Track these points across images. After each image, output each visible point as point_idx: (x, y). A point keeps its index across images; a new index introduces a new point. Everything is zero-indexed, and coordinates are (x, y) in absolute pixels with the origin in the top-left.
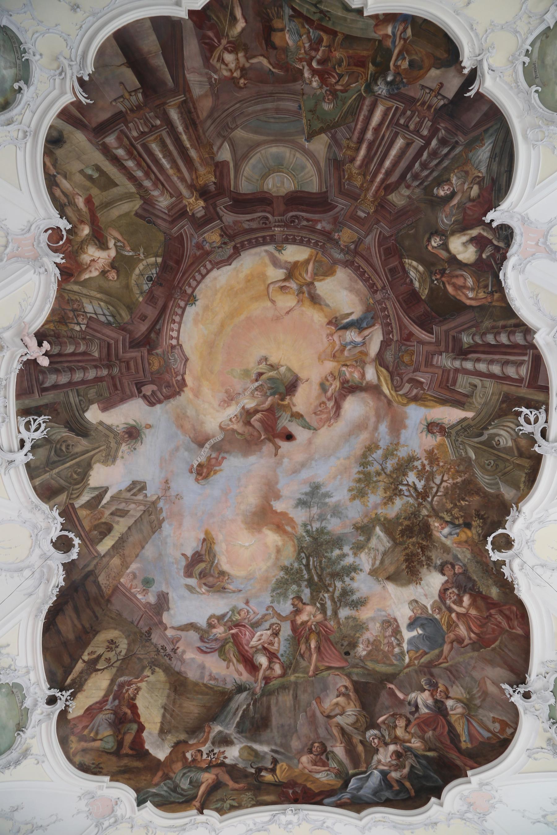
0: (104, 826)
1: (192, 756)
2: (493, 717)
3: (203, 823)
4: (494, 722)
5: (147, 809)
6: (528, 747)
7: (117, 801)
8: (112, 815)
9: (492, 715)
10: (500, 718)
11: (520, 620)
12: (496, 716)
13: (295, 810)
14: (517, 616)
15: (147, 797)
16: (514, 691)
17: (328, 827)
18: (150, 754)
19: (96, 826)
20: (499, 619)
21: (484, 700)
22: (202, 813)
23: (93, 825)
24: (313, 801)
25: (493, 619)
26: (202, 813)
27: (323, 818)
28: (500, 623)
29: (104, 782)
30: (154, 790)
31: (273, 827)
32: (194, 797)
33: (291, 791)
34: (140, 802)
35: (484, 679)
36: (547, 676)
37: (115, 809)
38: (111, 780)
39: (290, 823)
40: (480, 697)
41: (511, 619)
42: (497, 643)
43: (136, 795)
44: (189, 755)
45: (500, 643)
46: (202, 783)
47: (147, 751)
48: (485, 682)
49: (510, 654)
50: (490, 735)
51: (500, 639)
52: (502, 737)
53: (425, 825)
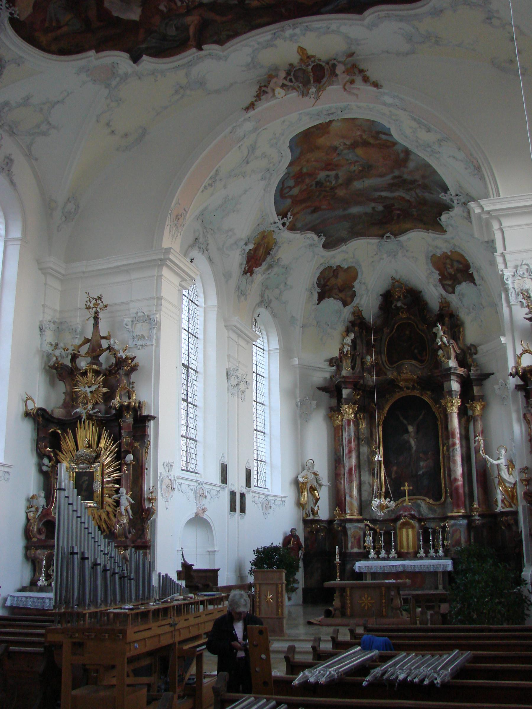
1: (166, 7)
3: (206, 56)
7: (114, 66)
13: (293, 25)
17: (333, 31)
18: (122, 19)
26: (201, 49)
29: (91, 56)
30: (144, 46)
31: (278, 42)
32: (188, 39)
33: (283, 10)
34: (136, 59)
38: (97, 52)
39: (295, 35)
44: (162, 7)
46: (189, 26)
47: (117, 18)
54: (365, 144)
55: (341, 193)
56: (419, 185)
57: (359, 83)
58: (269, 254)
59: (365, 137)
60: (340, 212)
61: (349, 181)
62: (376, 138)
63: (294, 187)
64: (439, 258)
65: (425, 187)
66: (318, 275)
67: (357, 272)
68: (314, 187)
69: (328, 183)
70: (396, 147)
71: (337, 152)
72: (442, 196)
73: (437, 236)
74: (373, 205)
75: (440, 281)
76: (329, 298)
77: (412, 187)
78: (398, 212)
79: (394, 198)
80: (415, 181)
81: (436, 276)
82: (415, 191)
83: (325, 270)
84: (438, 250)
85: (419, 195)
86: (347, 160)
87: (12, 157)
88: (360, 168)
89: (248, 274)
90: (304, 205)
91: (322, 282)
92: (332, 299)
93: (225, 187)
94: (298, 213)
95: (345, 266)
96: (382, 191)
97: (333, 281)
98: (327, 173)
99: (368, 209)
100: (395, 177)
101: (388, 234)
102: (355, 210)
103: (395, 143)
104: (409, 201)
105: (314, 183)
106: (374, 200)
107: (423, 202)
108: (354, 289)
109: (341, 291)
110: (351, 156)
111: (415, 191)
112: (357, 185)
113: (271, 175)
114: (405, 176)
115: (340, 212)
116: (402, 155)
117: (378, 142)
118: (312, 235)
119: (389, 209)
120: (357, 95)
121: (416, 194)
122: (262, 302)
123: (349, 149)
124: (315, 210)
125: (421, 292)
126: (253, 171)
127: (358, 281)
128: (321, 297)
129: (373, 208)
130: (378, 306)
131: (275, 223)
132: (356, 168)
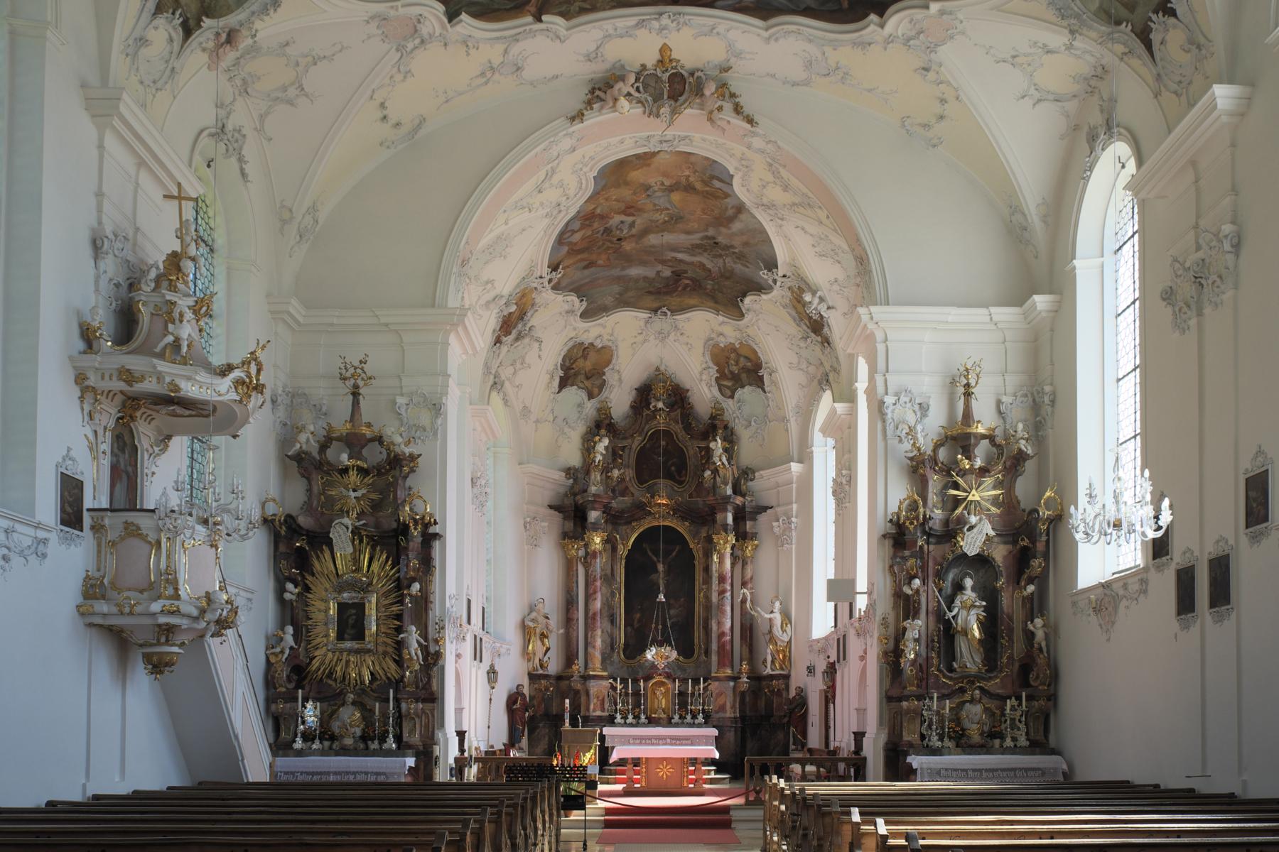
0: (408, 50)
5: (463, 24)
8: (416, 36)
15: (461, 8)
19: (397, 50)
22: (540, 20)
23: (393, 50)
24: (700, 3)
27: (711, 23)
37: (418, 28)
43: (444, 8)
53: (855, 43)
54: (689, 188)
55: (628, 246)
56: (734, 253)
57: (728, 114)
58: (522, 319)
59: (691, 179)
60: (616, 272)
61: (645, 232)
62: (705, 183)
63: (577, 231)
64: (723, 350)
65: (741, 257)
66: (563, 354)
67: (612, 356)
68: (599, 235)
69: (618, 232)
70: (728, 200)
71: (648, 193)
72: (764, 274)
73: (726, 320)
74: (660, 267)
75: (717, 379)
76: (572, 385)
77: (723, 253)
78: (687, 282)
79: (692, 263)
80: (732, 247)
81: (713, 371)
82: (724, 260)
83: (574, 346)
84: (722, 339)
85: (728, 265)
86: (655, 205)
87: (244, 132)
88: (666, 219)
89: (498, 345)
90: (579, 257)
91: (567, 364)
92: (576, 387)
93: (506, 223)
94: (568, 267)
95: (599, 344)
96: (679, 252)
97: (580, 363)
98: (623, 218)
99: (649, 272)
100: (707, 237)
101: (665, 309)
102: (635, 271)
103: (727, 195)
104: (710, 271)
105: (602, 229)
106: (663, 262)
107: (727, 275)
108: (604, 377)
109: (588, 378)
110: (662, 202)
111: (724, 260)
112: (653, 239)
113: (560, 211)
114: (720, 239)
115: (616, 272)
116: (730, 212)
117: (708, 189)
118: (573, 298)
119: (678, 275)
120: (724, 130)
121: (725, 263)
122: (495, 383)
123: (664, 191)
124: (591, 264)
125: (688, 390)
126: (542, 204)
127: (611, 366)
128: (563, 383)
129: (658, 272)
130: (629, 403)
131: (541, 277)
132: (661, 217)
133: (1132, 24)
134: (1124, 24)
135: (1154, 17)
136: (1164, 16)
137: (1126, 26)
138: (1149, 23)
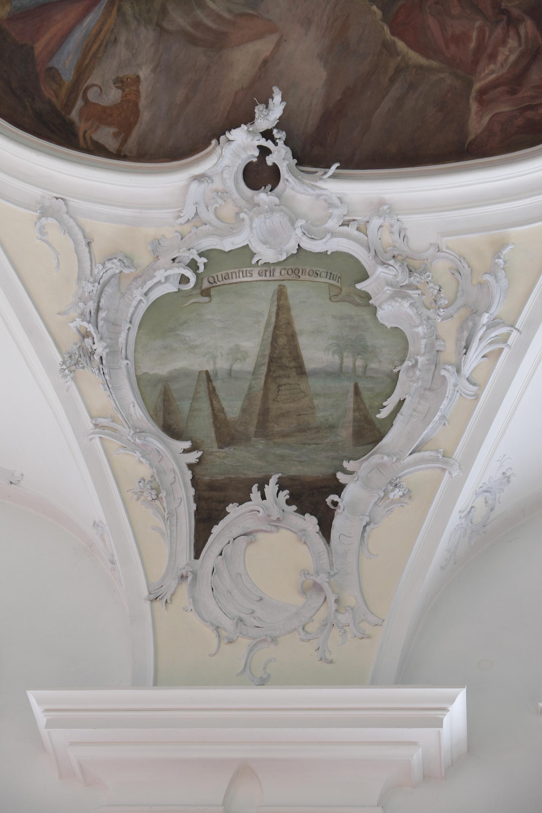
2: (137, 79)
4: (120, 83)
6: (74, 203)
9: (144, 73)
10: (143, 102)
11: (520, 121)
12: (144, 88)
14: (531, 108)
16: (267, 134)
20: (503, 53)
21: (192, 40)
25: (499, 31)
28: (492, 57)
35: (273, 30)
36: (351, 230)
40: (198, 25)
41: (513, 92)
42: (415, 58)
45: (420, 68)
48: (259, 36)
49: (387, 104)
50: (68, 76)
51: (434, 63)
52: (74, 115)
133: (200, 458)
134: (187, 445)
135: (271, 489)
136: (288, 503)
137: (186, 451)
138: (255, 488)
